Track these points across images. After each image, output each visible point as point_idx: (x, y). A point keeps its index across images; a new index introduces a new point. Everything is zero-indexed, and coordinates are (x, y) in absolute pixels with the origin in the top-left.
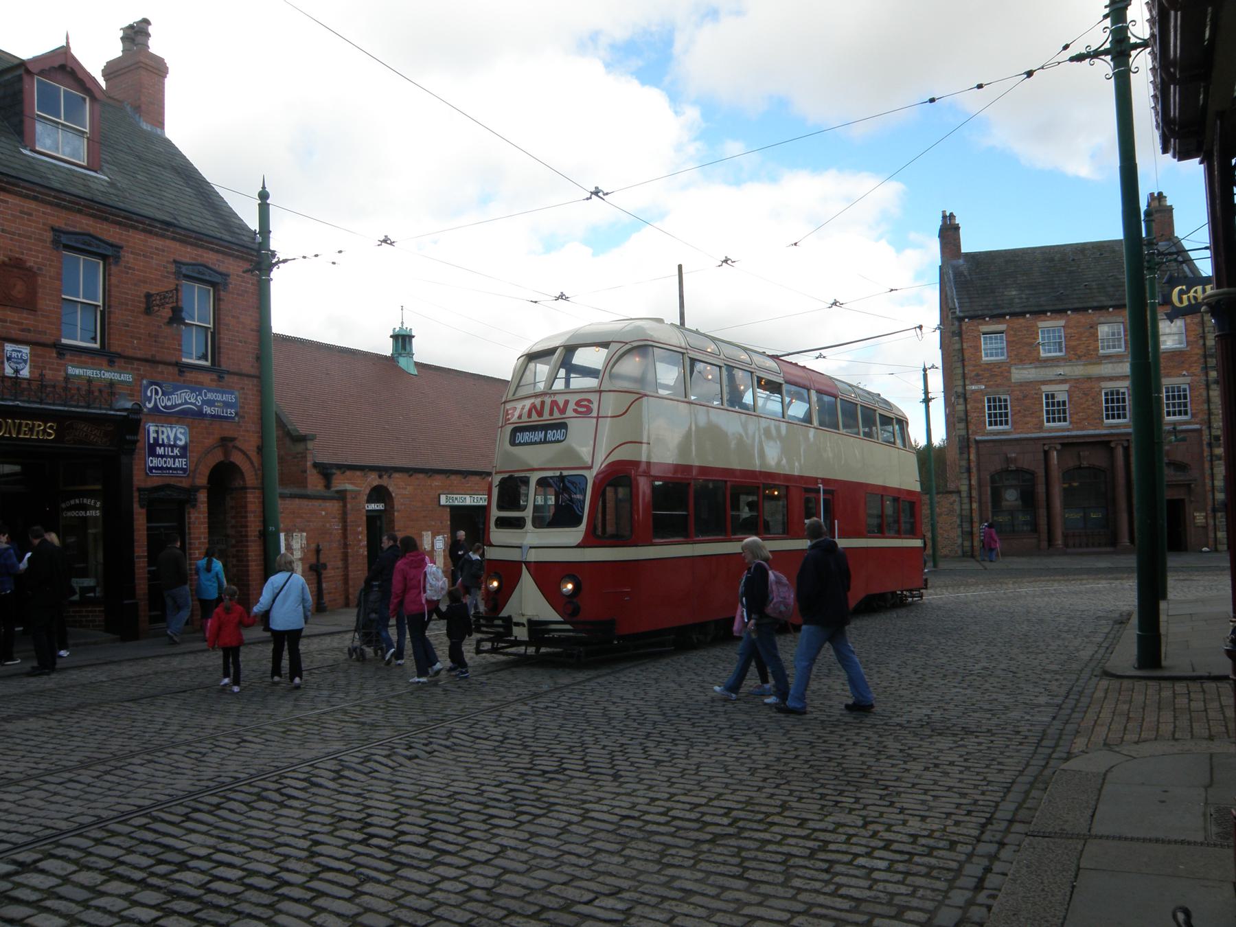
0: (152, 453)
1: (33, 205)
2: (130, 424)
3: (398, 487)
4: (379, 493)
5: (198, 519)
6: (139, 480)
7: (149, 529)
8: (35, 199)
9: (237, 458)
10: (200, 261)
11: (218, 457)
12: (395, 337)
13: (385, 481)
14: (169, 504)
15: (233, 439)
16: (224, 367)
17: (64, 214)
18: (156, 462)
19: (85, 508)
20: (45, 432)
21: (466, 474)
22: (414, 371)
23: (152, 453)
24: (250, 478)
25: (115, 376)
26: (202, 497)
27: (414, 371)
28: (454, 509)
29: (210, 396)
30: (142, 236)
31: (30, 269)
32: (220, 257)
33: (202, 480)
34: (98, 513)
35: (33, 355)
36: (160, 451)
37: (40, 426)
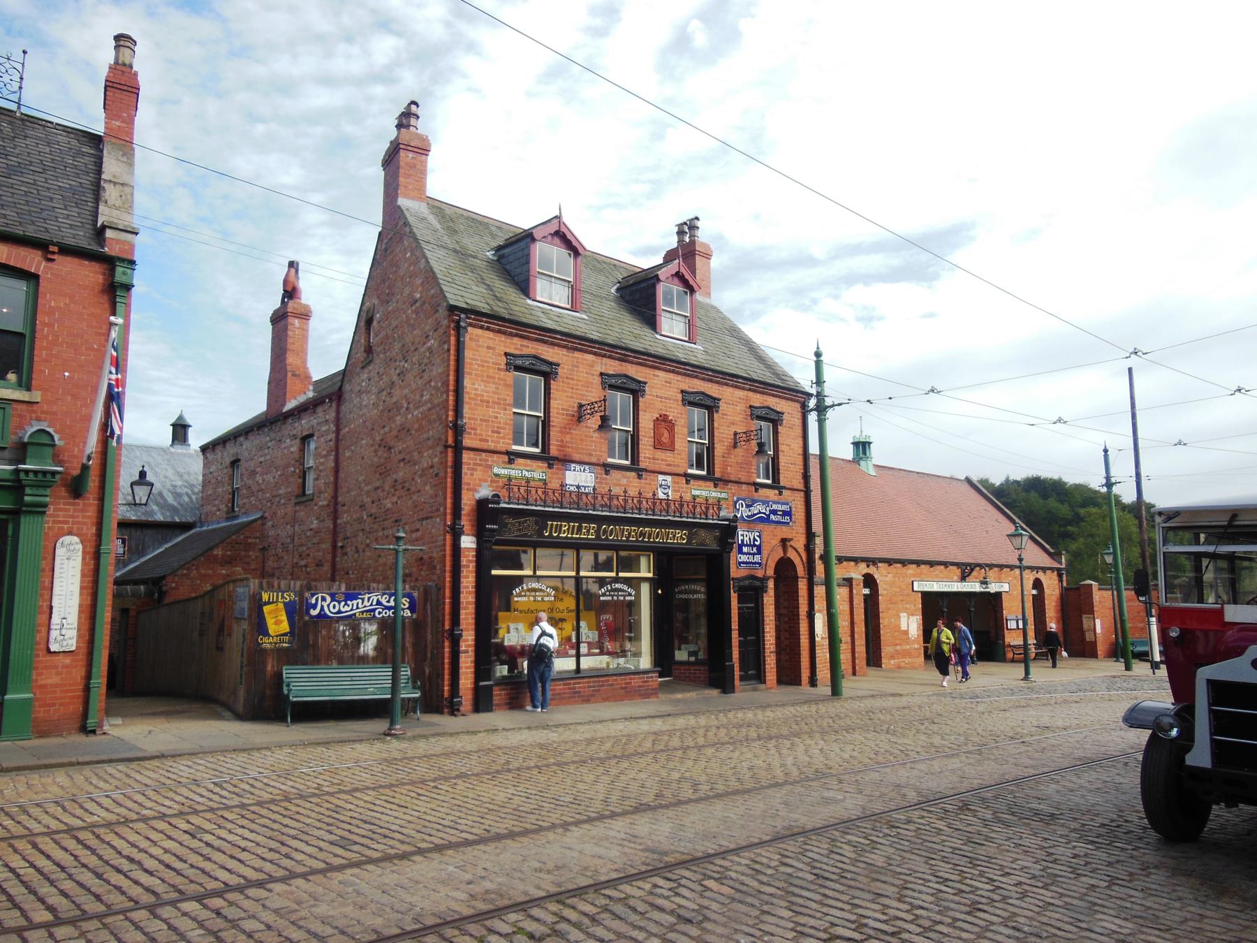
0: (741, 552)
1: (671, 376)
2: (727, 531)
3: (883, 575)
4: (869, 581)
5: (769, 600)
6: (735, 572)
7: (739, 608)
8: (673, 372)
9: (791, 554)
10: (766, 404)
11: (779, 554)
12: (856, 444)
13: (872, 570)
14: (752, 591)
15: (791, 540)
16: (782, 484)
17: (688, 380)
18: (744, 558)
19: (696, 592)
20: (678, 538)
21: (932, 564)
22: (872, 472)
23: (741, 552)
24: (801, 571)
25: (719, 495)
26: (771, 584)
27: (872, 472)
28: (926, 596)
29: (775, 507)
30: (730, 390)
31: (670, 422)
32: (777, 400)
33: (770, 572)
34: (702, 596)
35: (674, 482)
36: (745, 549)
37: (679, 533)
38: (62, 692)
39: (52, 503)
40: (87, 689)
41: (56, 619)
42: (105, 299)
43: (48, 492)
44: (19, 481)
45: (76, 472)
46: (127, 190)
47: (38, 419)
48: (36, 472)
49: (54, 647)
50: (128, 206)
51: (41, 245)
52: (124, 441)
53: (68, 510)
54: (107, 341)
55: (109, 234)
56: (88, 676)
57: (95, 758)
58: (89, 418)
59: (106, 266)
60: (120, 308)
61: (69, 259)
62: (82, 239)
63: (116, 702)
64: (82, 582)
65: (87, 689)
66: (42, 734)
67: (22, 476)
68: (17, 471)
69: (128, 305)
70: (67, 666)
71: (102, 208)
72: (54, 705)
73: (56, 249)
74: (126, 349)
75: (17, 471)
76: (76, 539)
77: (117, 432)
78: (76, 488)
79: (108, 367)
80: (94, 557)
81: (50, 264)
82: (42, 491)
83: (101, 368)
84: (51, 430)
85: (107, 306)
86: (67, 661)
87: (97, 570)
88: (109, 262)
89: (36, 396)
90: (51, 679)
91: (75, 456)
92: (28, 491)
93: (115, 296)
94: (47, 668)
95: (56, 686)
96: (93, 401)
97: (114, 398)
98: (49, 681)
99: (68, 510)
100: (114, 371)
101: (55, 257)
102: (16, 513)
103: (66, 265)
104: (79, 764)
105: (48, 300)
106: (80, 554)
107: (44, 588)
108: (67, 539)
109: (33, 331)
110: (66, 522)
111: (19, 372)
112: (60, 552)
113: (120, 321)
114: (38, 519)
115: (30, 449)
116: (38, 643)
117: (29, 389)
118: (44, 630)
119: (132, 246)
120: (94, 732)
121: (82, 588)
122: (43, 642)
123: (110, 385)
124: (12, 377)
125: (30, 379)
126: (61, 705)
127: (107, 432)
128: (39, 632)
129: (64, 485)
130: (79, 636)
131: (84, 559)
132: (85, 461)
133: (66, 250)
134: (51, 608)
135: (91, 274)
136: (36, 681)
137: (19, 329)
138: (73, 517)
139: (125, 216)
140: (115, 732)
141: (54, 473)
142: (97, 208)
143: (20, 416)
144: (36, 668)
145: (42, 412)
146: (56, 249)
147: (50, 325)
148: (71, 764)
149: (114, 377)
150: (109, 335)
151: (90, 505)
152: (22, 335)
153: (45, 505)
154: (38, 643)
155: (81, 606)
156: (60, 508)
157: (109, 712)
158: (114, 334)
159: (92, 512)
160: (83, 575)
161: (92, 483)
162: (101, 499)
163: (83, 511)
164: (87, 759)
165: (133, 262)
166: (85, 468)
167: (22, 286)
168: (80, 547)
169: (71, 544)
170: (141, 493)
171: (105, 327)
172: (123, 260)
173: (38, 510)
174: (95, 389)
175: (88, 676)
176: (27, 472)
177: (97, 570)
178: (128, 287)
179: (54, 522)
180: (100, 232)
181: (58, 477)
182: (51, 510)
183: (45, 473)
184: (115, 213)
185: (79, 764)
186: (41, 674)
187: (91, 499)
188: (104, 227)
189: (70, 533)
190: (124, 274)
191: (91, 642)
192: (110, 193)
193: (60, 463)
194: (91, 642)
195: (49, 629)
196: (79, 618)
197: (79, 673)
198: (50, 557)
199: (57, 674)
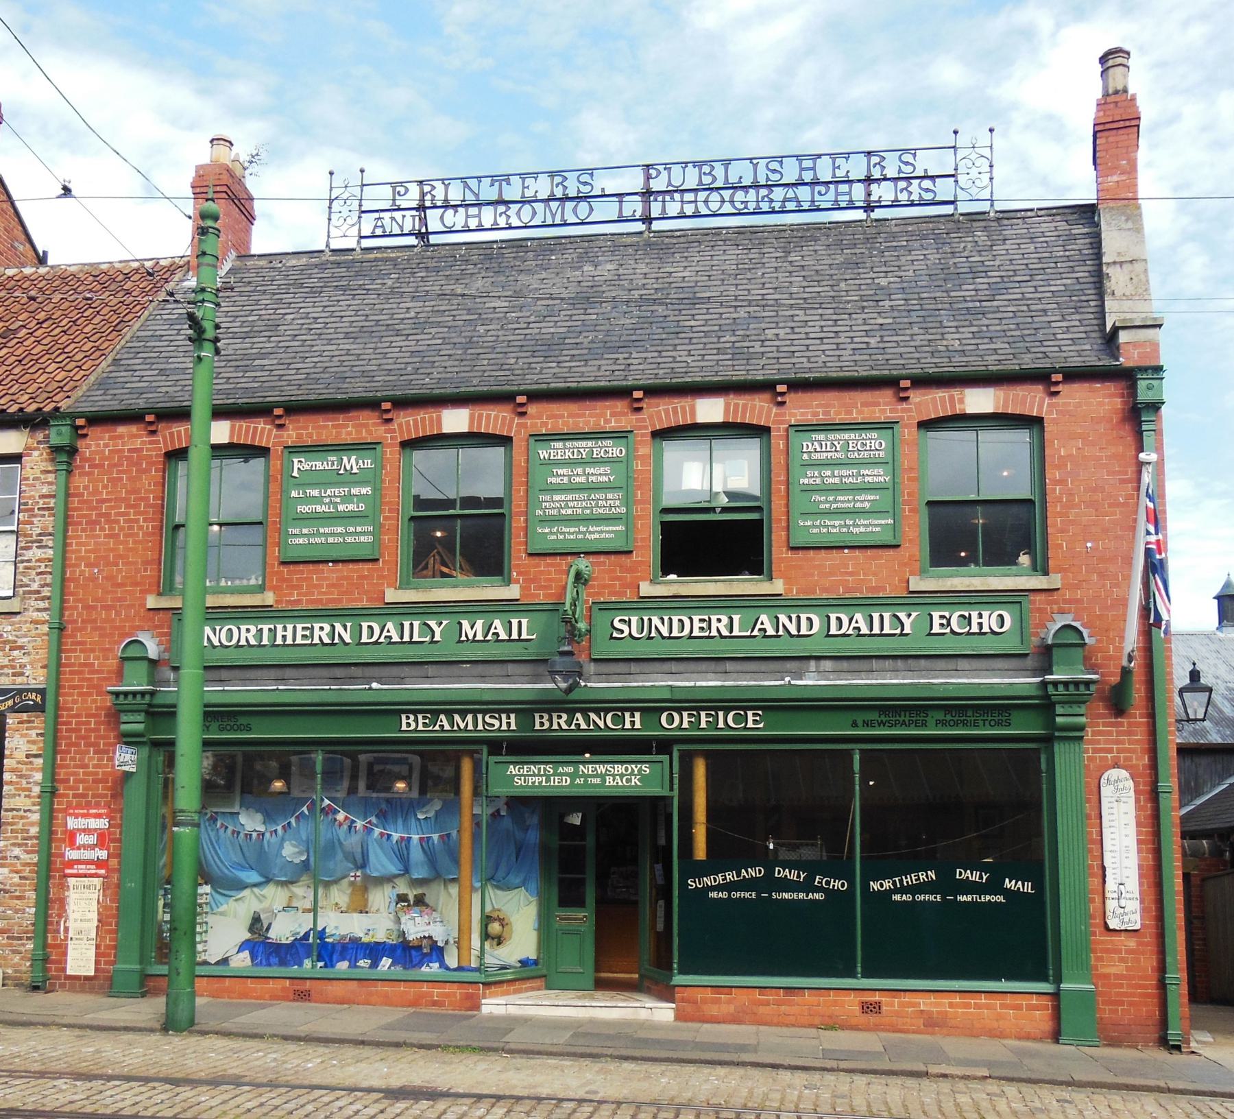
38: (1129, 986)
39: (1092, 725)
40: (1162, 985)
41: (1111, 885)
42: (1126, 431)
43: (1082, 710)
44: (1047, 697)
45: (1115, 680)
46: (1138, 267)
47: (1062, 612)
48: (1066, 684)
49: (1113, 924)
50: (1142, 292)
51: (1039, 377)
52: (1174, 628)
53: (1110, 733)
54: (1138, 489)
55: (1123, 337)
56: (1162, 968)
57: (1191, 1087)
58: (1124, 603)
59: (1123, 384)
60: (1148, 439)
61: (1076, 386)
62: (1088, 354)
63: (1205, 1010)
64: (1139, 833)
65: (1162, 985)
66: (1113, 1043)
67: (1050, 689)
68: (1044, 684)
69: (1158, 433)
70: (1129, 951)
71: (1108, 304)
72: (1122, 1003)
73: (1059, 377)
74: (1163, 496)
75: (1044, 684)
76: (1124, 774)
77: (1165, 616)
78: (1117, 702)
79: (1143, 524)
80: (1151, 796)
81: (1054, 400)
82: (1076, 709)
83: (1134, 529)
84: (1077, 624)
85: (1130, 439)
86: (1132, 943)
87: (1156, 816)
88: (1127, 377)
89: (1054, 581)
90: (1114, 968)
91: (1110, 658)
92: (1059, 709)
93: (1140, 423)
94: (1107, 951)
95: (1117, 976)
96: (1128, 578)
97: (1155, 567)
98: (1113, 970)
99: (1110, 733)
100: (1152, 529)
101: (1060, 388)
102: (1048, 740)
103: (1075, 396)
104: (1169, 1090)
105: (1057, 449)
106: (1132, 793)
107: (1092, 842)
108: (1114, 773)
109: (1044, 494)
110: (1110, 751)
111: (1032, 552)
112: (1106, 791)
113: (1153, 457)
114: (1074, 747)
115: (1056, 653)
116: (1092, 917)
117: (1046, 573)
118: (1098, 899)
119: (1155, 346)
120: (1178, 1048)
121: (1139, 842)
122: (1100, 912)
123: (1148, 552)
124: (1024, 559)
125: (1046, 559)
126: (1131, 1004)
127: (1151, 620)
128: (1093, 900)
129: (1102, 699)
130: (1144, 910)
131: (1137, 801)
132: (1125, 663)
133: (1073, 375)
134: (1104, 869)
135: (1102, 401)
136: (1096, 968)
137: (1026, 495)
138: (1117, 742)
139: (1140, 306)
140: (1207, 1052)
141: (1088, 683)
142: (1103, 306)
143: (1040, 610)
144: (1094, 951)
145: (1065, 601)
146: (1059, 377)
147: (1062, 482)
148: (1159, 1090)
149: (1153, 538)
150: (1139, 480)
151: (1138, 724)
152: (1030, 502)
153: (1081, 728)
154: (1092, 917)
155: (1140, 867)
156: (1102, 733)
157: (1196, 1023)
158: (1146, 478)
159: (1141, 735)
160: (1139, 824)
161: (1137, 693)
162: (1152, 716)
163: (1129, 733)
164: (1181, 1085)
165: (1159, 369)
166: (1126, 672)
167: (1022, 437)
168: (1131, 783)
169: (1118, 780)
170: (1196, 704)
171: (1131, 470)
172: (1145, 369)
173: (1074, 734)
174: (1129, 561)
175: (1162, 968)
176: (1055, 684)
177: (1156, 816)
178: (1155, 406)
179: (1096, 751)
180: (1110, 340)
181: (1093, 688)
182: (1089, 734)
183: (1077, 684)
184: (1127, 305)
185: (1169, 1090)
186: (1099, 959)
187: (1137, 715)
188: (1116, 330)
189: (1116, 765)
190: (1149, 388)
191: (1160, 918)
192: (1117, 279)
193: (1092, 668)
194: (1160, 918)
195: (1104, 898)
196: (1141, 884)
197: (1149, 962)
198: (1094, 798)
199: (1122, 960)
